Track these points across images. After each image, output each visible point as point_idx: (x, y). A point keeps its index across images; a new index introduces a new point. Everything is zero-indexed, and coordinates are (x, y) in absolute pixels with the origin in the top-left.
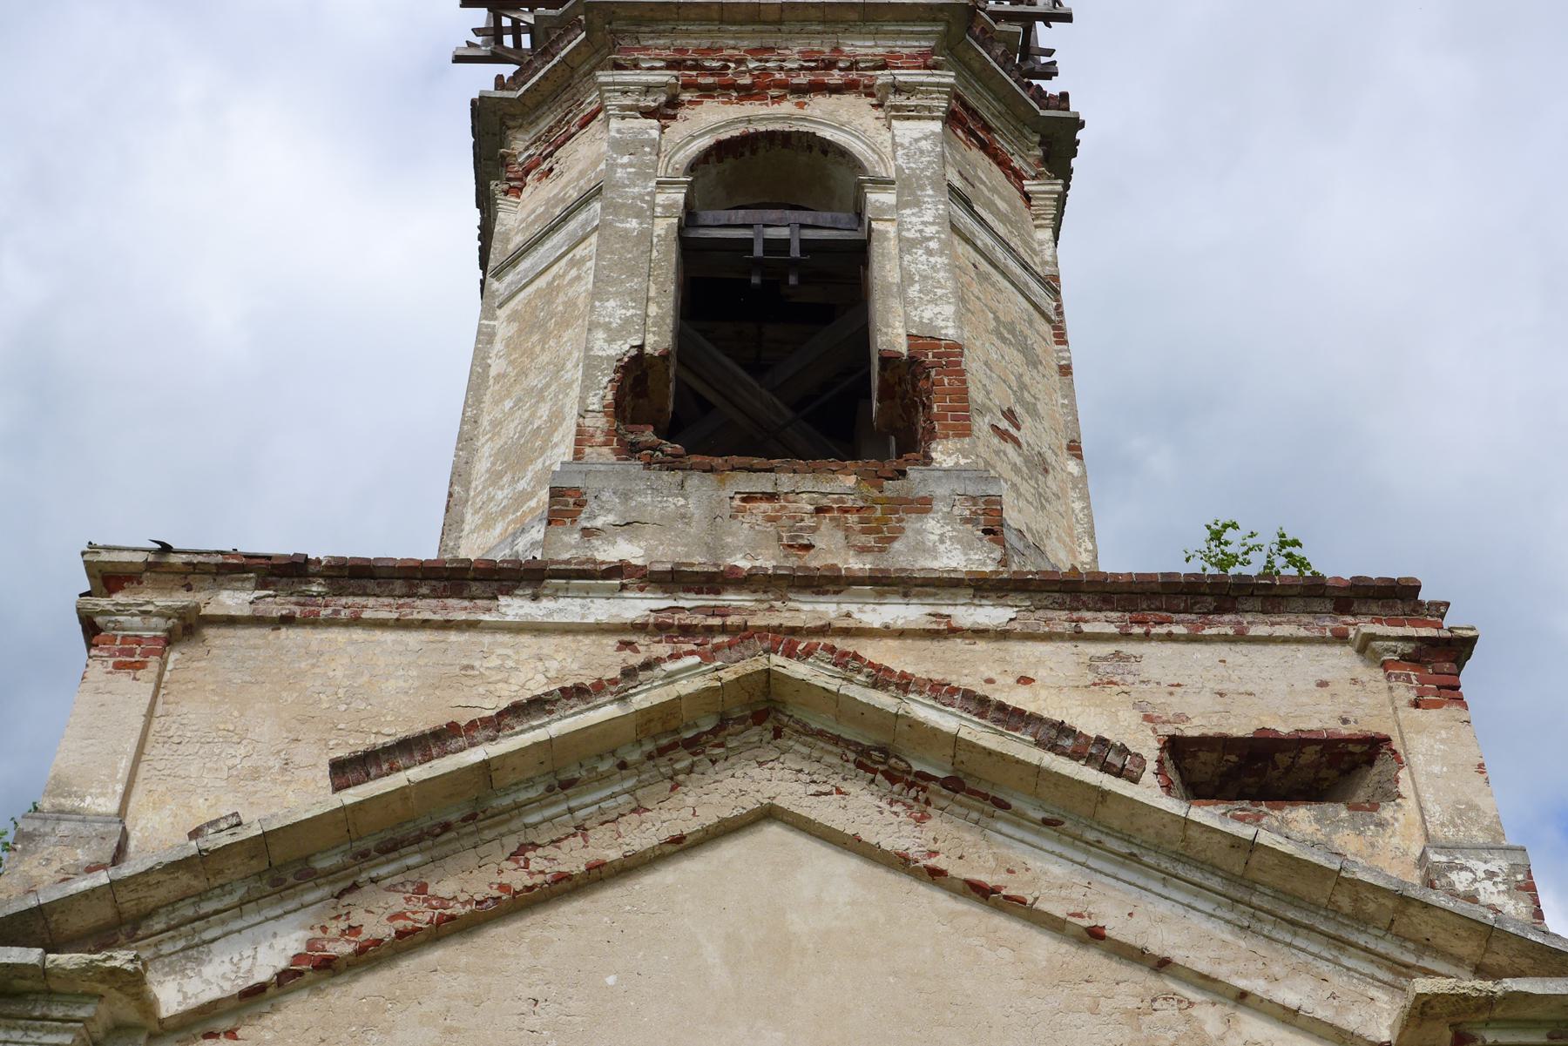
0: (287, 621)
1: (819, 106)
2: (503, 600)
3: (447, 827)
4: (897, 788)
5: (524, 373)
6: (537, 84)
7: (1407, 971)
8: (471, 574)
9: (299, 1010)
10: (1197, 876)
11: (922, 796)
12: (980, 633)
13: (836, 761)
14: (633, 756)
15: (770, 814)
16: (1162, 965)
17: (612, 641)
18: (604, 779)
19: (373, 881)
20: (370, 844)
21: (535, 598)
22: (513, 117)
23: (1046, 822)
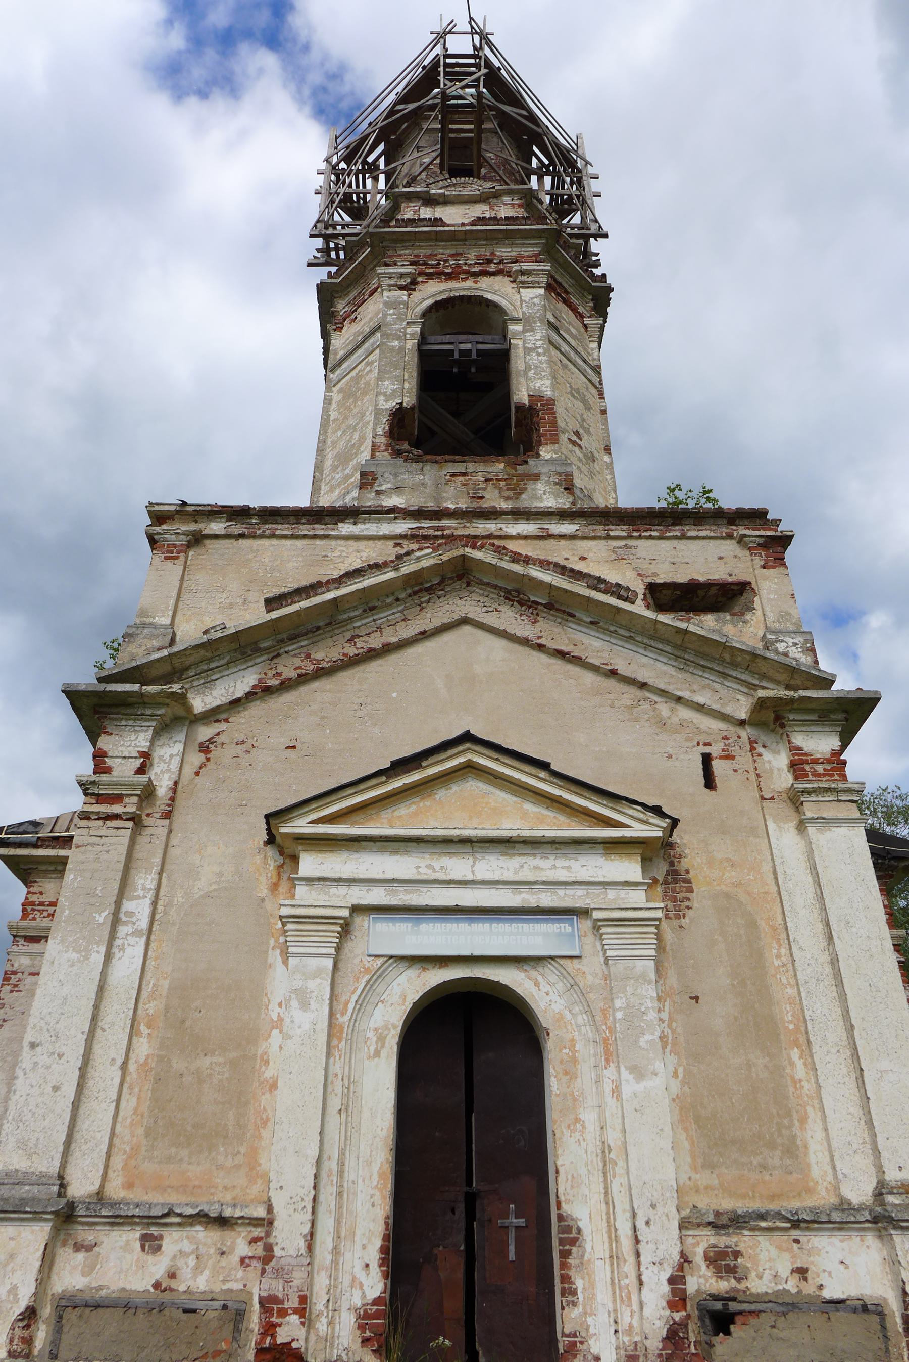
0: (242, 536)
2: (340, 525)
3: (318, 628)
4: (523, 608)
5: (346, 418)
6: (347, 275)
7: (755, 687)
8: (325, 513)
9: (256, 709)
10: (660, 646)
11: (535, 612)
12: (562, 537)
13: (495, 596)
14: (402, 595)
15: (465, 621)
16: (643, 686)
17: (391, 543)
18: (389, 606)
19: (287, 652)
20: (285, 636)
21: (355, 523)
22: (337, 292)
23: (591, 623)
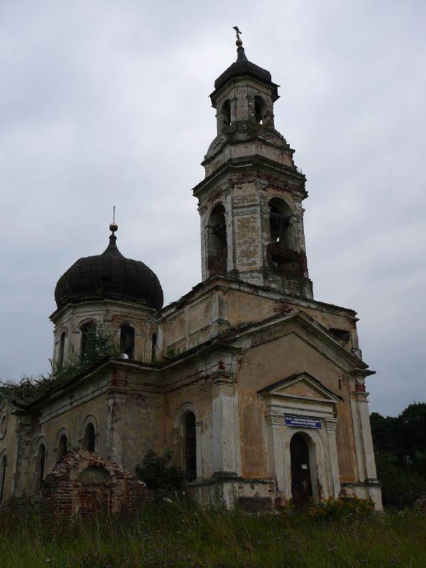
5: (244, 236)
12: (312, 309)
15: (294, 332)
16: (328, 358)
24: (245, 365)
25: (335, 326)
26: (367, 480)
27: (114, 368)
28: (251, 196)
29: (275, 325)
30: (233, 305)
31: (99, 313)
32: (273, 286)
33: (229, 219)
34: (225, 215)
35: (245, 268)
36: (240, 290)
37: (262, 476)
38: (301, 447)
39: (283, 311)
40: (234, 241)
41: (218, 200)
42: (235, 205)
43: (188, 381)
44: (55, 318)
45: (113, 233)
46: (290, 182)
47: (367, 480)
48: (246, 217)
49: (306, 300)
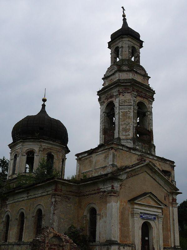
1: (145, 100)
5: (124, 121)
15: (146, 171)
16: (161, 185)
24: (123, 187)
25: (165, 169)
26: (175, 246)
27: (56, 183)
28: (128, 100)
29: (138, 168)
30: (119, 157)
31: (37, 146)
32: (138, 147)
33: (117, 111)
34: (115, 109)
35: (124, 137)
36: (122, 149)
37: (128, 242)
38: (146, 228)
39: (141, 160)
40: (119, 122)
41: (110, 100)
42: (120, 104)
43: (93, 192)
44: (11, 146)
45: (44, 103)
46: (147, 94)
47: (175, 246)
48: (126, 111)
49: (152, 155)
